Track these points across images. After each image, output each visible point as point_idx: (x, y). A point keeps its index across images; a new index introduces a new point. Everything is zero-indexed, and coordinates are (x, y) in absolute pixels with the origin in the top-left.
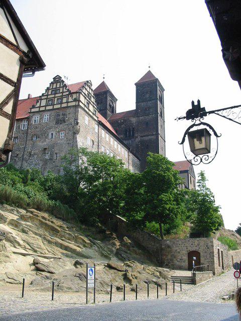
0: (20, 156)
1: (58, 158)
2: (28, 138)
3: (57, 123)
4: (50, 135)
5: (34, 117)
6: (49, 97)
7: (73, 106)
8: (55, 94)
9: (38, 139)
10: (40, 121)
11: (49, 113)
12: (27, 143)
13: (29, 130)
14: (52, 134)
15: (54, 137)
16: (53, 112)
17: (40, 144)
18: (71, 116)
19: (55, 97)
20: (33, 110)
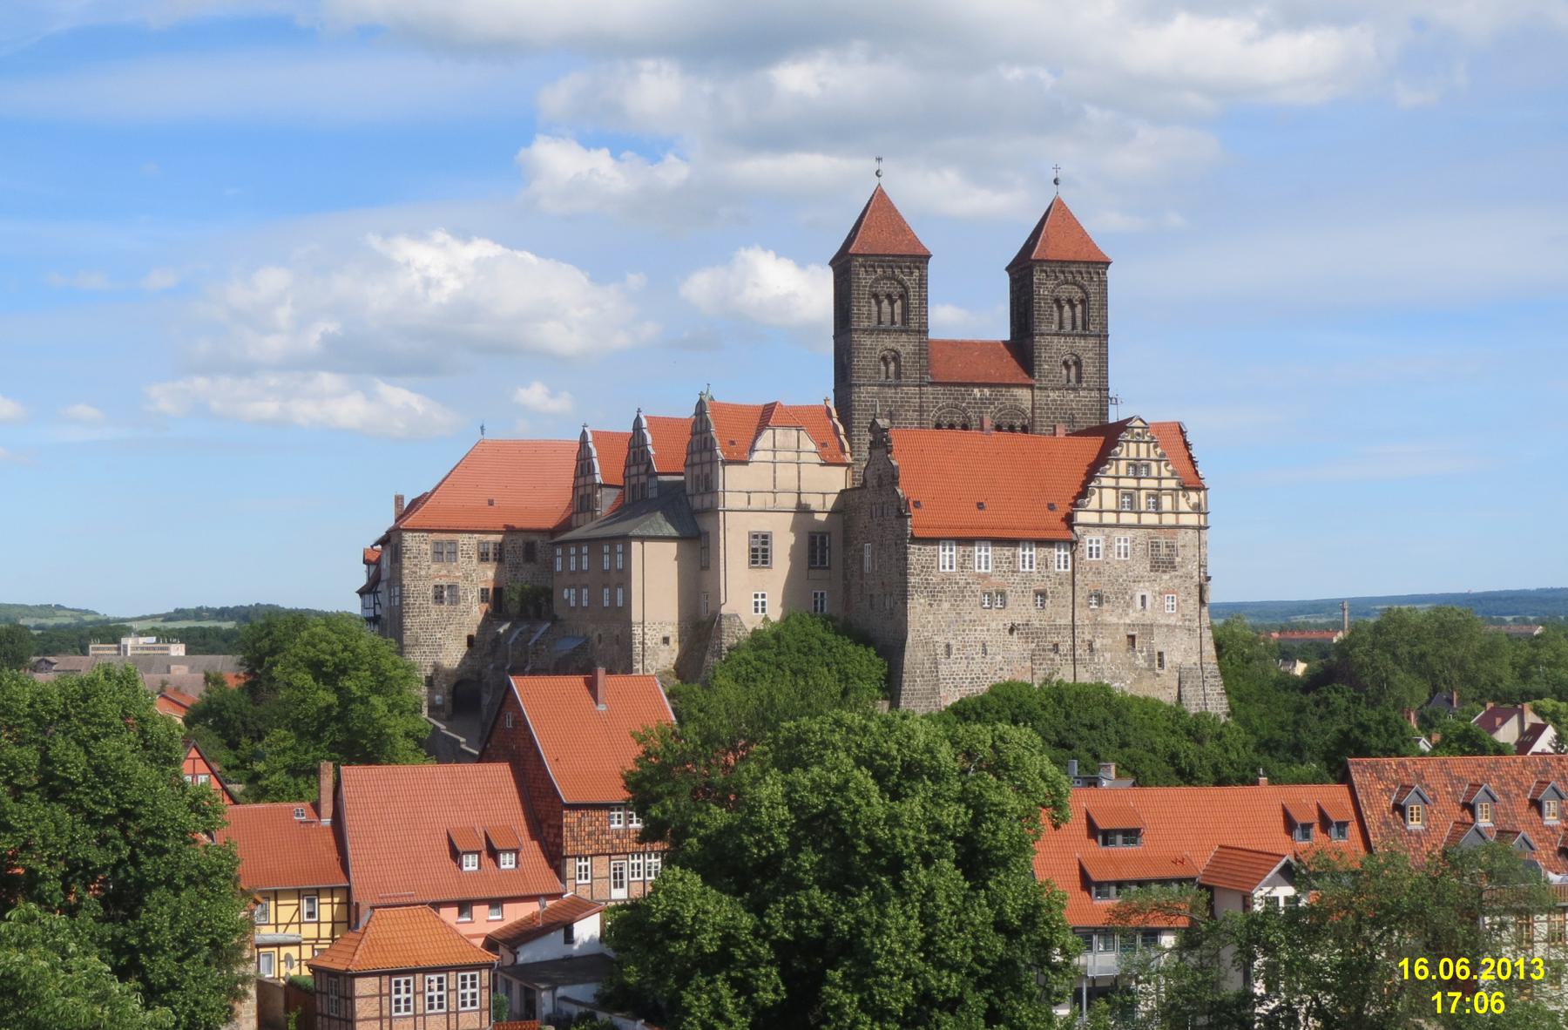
0: (1065, 647)
1: (1167, 665)
4: (1139, 601)
5: (1087, 538)
6: (1123, 483)
7: (1193, 528)
8: (1139, 479)
9: (1105, 606)
11: (1130, 534)
13: (1078, 576)
14: (1143, 597)
16: (1141, 532)
17: (1114, 620)
19: (1139, 489)
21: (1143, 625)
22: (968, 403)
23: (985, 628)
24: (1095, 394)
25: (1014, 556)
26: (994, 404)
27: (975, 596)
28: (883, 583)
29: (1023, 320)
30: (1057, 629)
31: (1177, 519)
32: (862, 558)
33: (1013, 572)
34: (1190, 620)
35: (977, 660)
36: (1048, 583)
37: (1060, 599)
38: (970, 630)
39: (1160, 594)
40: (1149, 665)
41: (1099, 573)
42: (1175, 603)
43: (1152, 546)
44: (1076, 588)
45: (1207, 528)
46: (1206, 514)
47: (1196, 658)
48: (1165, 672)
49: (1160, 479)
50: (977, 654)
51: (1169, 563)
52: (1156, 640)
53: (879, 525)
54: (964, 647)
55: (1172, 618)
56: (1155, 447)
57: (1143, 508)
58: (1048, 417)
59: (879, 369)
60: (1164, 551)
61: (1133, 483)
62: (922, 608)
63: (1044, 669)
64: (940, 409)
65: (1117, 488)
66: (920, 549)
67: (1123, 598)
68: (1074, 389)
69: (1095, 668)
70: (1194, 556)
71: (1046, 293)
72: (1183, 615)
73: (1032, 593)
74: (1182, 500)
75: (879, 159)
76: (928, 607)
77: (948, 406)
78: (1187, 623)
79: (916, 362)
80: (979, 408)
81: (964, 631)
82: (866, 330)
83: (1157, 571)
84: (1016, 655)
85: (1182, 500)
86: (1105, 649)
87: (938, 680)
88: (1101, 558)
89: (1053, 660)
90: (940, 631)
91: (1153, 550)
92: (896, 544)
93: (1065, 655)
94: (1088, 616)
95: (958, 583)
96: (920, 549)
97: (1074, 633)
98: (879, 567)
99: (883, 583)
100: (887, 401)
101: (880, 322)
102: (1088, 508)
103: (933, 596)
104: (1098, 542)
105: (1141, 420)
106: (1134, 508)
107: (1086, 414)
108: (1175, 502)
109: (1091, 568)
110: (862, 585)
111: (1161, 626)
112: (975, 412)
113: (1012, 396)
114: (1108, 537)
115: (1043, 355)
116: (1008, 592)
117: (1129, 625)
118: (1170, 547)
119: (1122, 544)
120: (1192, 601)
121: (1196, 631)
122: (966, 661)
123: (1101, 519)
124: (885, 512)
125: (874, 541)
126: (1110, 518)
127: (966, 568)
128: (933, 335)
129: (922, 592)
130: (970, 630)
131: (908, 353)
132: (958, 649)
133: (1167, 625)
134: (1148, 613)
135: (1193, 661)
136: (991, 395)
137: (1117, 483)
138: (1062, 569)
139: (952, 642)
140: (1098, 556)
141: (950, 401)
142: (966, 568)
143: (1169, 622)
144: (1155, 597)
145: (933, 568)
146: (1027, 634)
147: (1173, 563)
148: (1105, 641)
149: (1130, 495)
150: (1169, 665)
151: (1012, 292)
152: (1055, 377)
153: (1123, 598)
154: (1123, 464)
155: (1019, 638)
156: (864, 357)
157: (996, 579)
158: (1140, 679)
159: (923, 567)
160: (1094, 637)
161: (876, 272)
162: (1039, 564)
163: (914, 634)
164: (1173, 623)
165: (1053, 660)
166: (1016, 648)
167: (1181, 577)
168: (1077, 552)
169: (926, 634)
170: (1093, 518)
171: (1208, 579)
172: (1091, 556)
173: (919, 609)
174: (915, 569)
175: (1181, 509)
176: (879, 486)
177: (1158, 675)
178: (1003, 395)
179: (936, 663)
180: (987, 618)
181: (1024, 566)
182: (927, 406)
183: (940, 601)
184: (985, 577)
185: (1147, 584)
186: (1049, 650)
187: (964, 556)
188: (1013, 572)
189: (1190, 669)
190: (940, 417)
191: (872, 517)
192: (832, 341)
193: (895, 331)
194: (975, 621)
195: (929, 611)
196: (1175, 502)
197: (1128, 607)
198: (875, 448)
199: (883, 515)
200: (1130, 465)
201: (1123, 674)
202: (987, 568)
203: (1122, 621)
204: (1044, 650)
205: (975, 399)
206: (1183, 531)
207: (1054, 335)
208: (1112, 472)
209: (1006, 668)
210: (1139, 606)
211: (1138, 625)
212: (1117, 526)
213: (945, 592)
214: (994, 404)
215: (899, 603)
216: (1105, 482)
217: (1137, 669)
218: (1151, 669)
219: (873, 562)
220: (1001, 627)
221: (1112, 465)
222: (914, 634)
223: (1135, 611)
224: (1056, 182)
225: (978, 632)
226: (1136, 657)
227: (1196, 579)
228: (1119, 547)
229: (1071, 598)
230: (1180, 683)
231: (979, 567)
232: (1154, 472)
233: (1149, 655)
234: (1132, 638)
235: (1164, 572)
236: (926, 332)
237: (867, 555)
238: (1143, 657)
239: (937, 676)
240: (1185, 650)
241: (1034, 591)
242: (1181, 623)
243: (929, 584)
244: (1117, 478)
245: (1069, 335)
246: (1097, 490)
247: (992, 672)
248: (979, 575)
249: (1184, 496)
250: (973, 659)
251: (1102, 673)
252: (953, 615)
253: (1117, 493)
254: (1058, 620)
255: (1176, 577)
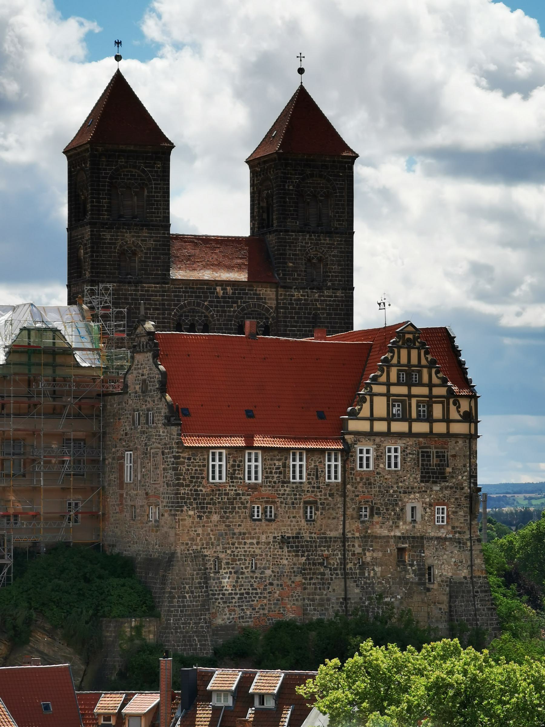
2: (349, 512)
3: (425, 479)
5: (358, 447)
6: (394, 390)
9: (376, 518)
10: (377, 466)
12: (347, 526)
13: (348, 486)
15: (418, 518)
16: (411, 441)
17: (385, 532)
18: (459, 463)
19: (410, 396)
20: (353, 425)
21: (413, 537)
22: (210, 302)
23: (255, 541)
24: (339, 293)
25: (284, 466)
26: (236, 302)
27: (245, 508)
28: (147, 494)
29: (265, 216)
30: (327, 541)
31: (448, 428)
32: (122, 466)
33: (284, 482)
34: (460, 533)
35: (247, 575)
36: (318, 494)
37: (331, 511)
38: (240, 543)
39: (431, 505)
40: (420, 579)
41: (370, 484)
42: (445, 515)
43: (423, 456)
44: (348, 499)
45: (479, 437)
46: (476, 422)
47: (465, 572)
48: (435, 586)
49: (431, 385)
50: (246, 568)
51: (440, 473)
52: (427, 553)
53: (143, 432)
54: (234, 560)
55: (442, 530)
56: (426, 353)
57: (414, 415)
58: (292, 318)
59: (119, 265)
60: (434, 461)
61: (403, 390)
62: (191, 520)
63: (315, 584)
64: (181, 307)
65: (388, 395)
66: (189, 459)
67: (394, 510)
68: (318, 288)
69: (365, 583)
70: (465, 466)
71: (291, 187)
72: (453, 528)
73: (302, 505)
74: (453, 408)
75: (118, 43)
76: (197, 520)
77: (189, 303)
78: (457, 535)
79: (159, 258)
80: (221, 307)
81: (233, 544)
82: (106, 224)
83: (427, 482)
84: (287, 569)
85: (453, 408)
86: (375, 562)
87: (208, 596)
88: (371, 468)
89: (323, 574)
90: (210, 545)
91: (423, 460)
92: (163, 453)
93: (336, 569)
94: (358, 528)
95: (227, 494)
96: (189, 459)
97: (344, 546)
98: (143, 476)
99: (147, 494)
100: (127, 299)
101: (121, 216)
102: (359, 416)
103: (202, 508)
104: (368, 451)
105: (411, 325)
106: (405, 417)
107: (331, 314)
108: (446, 411)
109: (361, 479)
110: (122, 495)
111: (432, 538)
112: (218, 311)
113: (255, 294)
114: (379, 446)
115: (288, 252)
116: (279, 504)
117: (400, 538)
118: (441, 456)
119: (393, 454)
120: (462, 513)
121: (465, 544)
122: (236, 576)
123: (372, 427)
124: (150, 418)
125: (136, 449)
126: (380, 427)
127: (236, 478)
128: (173, 230)
129: (191, 504)
130: (240, 543)
131: (149, 249)
132: (228, 563)
133: (438, 538)
134: (418, 526)
135: (464, 575)
136: (233, 293)
137: (388, 390)
138: (333, 480)
139: (222, 556)
140: (368, 466)
141: (192, 300)
142: (236, 478)
143: (440, 534)
144: (425, 509)
145: (203, 478)
146: (297, 547)
147: (444, 473)
148: (375, 555)
149: (402, 401)
150: (439, 579)
151: (252, 185)
152: (298, 275)
153: (394, 510)
154: (394, 371)
155: (289, 552)
156: (104, 252)
157: (266, 491)
158: (409, 595)
159: (192, 477)
160: (364, 550)
161: (117, 162)
162: (309, 474)
163: (183, 548)
164: (444, 536)
165: (323, 574)
166: (285, 562)
167: (451, 488)
168: (348, 462)
169: (195, 547)
170: (364, 426)
171: (479, 490)
172: (361, 466)
173: (188, 522)
174: (184, 479)
175: (451, 417)
176: (143, 392)
177: (428, 590)
178: (247, 294)
179: (206, 578)
180: (257, 531)
181: (294, 478)
182: (169, 305)
183: (210, 512)
184: (255, 487)
185: (418, 495)
186: (322, 564)
187: (233, 466)
188: (284, 482)
189: (460, 583)
190: (181, 316)
191: (134, 424)
192: (66, 233)
193: (136, 225)
194: (244, 534)
195: (198, 523)
196: (446, 411)
197: (399, 519)
198: (138, 352)
199: (147, 423)
200: (399, 371)
201: (393, 589)
202: (256, 478)
203: (392, 534)
204: (314, 564)
205: (217, 297)
206: (453, 441)
207: (299, 232)
208: (383, 379)
209: (275, 582)
210: (409, 518)
211: (408, 537)
212: (389, 434)
213: (214, 504)
214: (236, 302)
215: (166, 515)
216: (376, 389)
217: (407, 584)
218: (421, 583)
219: (135, 471)
220: (271, 540)
221: (383, 371)
222: (183, 548)
223: (405, 523)
224: (301, 71)
225: (248, 546)
226: (406, 571)
227: (467, 490)
228: (389, 457)
229: (341, 511)
230: (451, 597)
231: (249, 478)
232: (425, 379)
233: (420, 569)
234: (401, 551)
235: (435, 482)
236: (168, 226)
237: (127, 464)
238: (414, 571)
239: (206, 592)
240: (455, 564)
241: (306, 503)
242: (451, 536)
243: (199, 495)
244: (388, 384)
245: (313, 232)
246: (368, 398)
247: (262, 587)
248: (249, 486)
249: (455, 404)
250: (243, 573)
251: (373, 588)
252: (222, 527)
253: (388, 401)
254: (328, 533)
255: (446, 488)
